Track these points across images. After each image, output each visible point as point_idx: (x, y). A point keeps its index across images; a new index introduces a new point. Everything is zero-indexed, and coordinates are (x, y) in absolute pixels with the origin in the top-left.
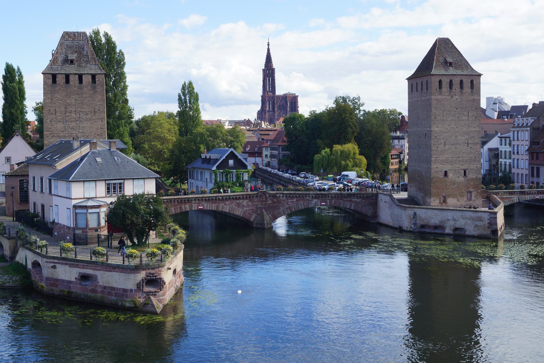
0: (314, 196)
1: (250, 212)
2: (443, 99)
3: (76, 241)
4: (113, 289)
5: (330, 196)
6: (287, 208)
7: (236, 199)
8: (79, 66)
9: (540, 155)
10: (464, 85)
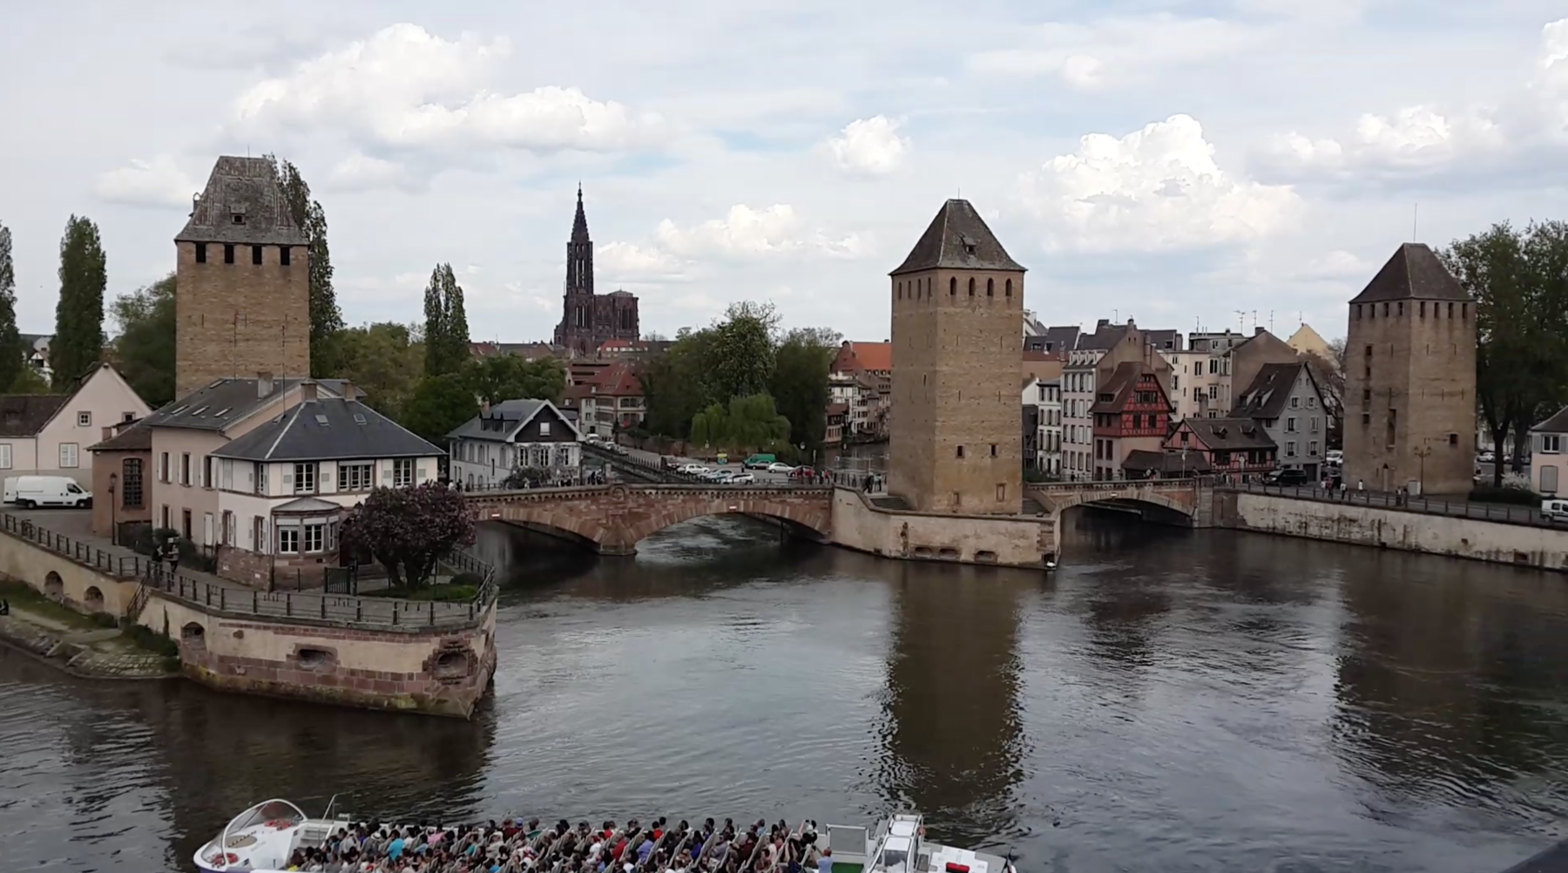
0: (716, 492)
2: (957, 313)
3: (276, 582)
4: (370, 674)
5: (746, 492)
6: (664, 517)
8: (255, 228)
9: (1113, 418)
10: (996, 289)
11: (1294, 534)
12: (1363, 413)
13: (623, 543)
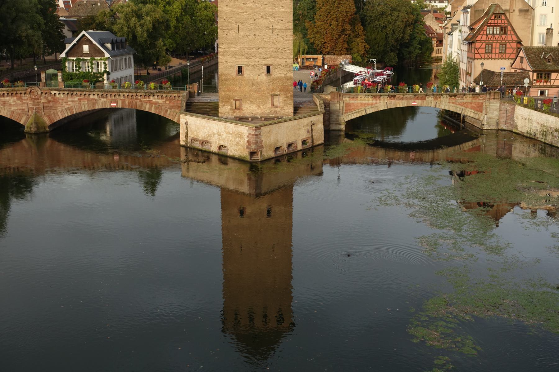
1: (19, 112)
6: (66, 109)
11: (539, 139)
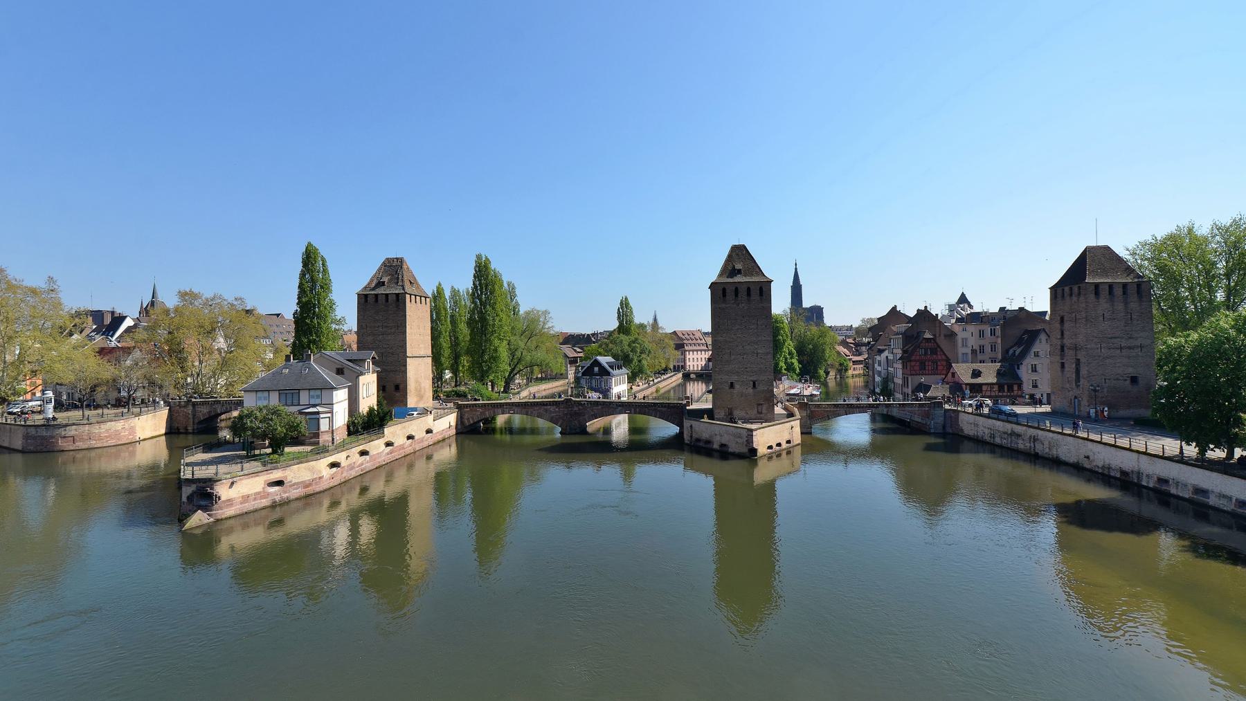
6: (592, 415)
7: (544, 405)
12: (1061, 361)
13: (568, 428)
